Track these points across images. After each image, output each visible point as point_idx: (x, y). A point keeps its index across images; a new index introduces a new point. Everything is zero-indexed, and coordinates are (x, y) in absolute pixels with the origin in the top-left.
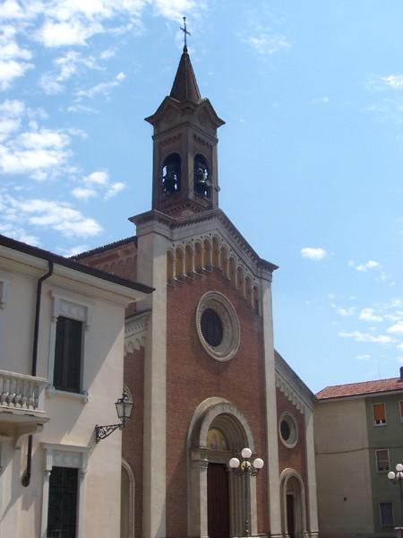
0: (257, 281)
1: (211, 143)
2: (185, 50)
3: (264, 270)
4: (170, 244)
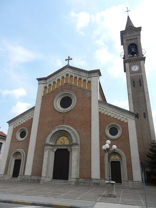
0: (89, 79)
1: (135, 37)
2: (128, 16)
3: (93, 74)
4: (45, 85)
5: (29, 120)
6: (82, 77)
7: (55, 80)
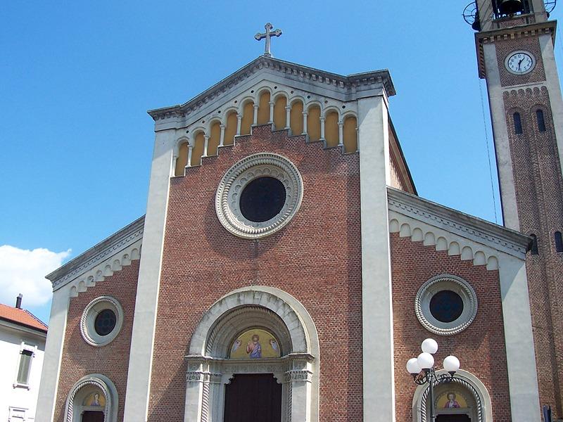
0: (349, 107)
3: (363, 87)
4: (182, 133)
5: (124, 268)
6: (323, 99)
7: (220, 115)
